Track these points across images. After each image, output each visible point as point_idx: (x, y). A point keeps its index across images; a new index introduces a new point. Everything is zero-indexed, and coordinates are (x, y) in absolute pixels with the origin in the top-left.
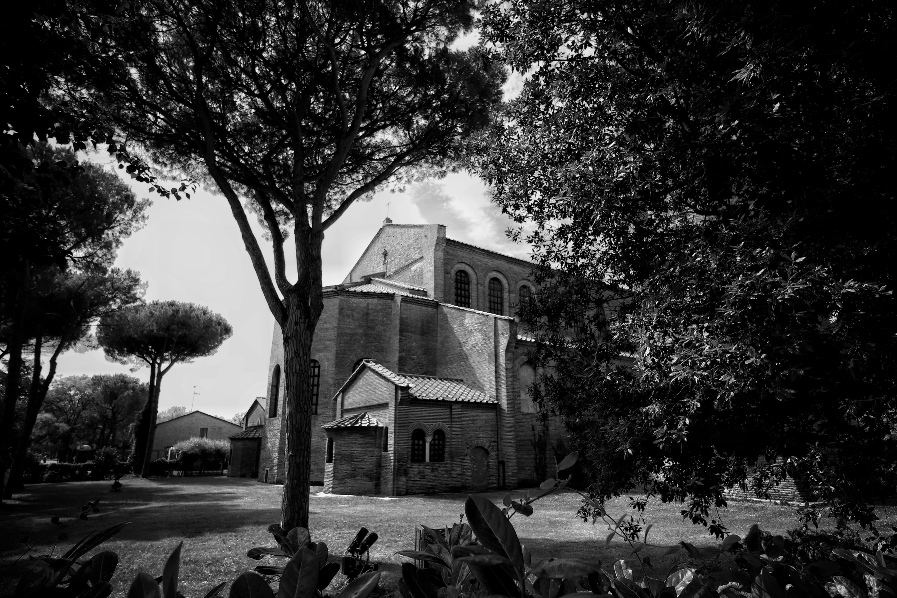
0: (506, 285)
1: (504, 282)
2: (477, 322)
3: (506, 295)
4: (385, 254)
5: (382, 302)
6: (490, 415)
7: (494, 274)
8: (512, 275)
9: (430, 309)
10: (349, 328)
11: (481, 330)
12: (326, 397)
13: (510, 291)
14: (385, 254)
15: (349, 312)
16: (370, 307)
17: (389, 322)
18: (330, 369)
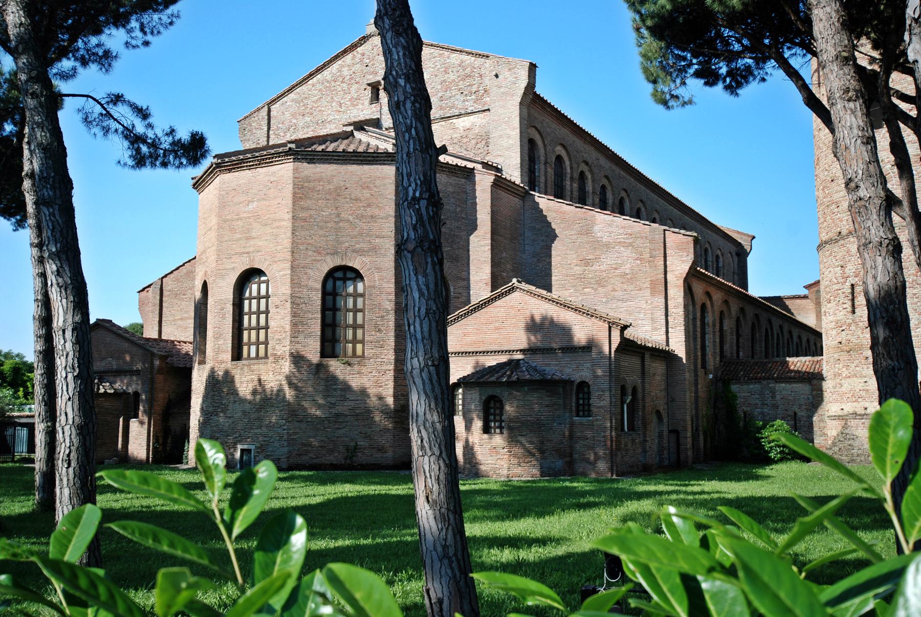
0: (569, 171)
2: (621, 231)
5: (453, 180)
7: (559, 150)
8: (575, 153)
9: (516, 200)
11: (631, 244)
12: (380, 330)
13: (572, 178)
17: (463, 215)
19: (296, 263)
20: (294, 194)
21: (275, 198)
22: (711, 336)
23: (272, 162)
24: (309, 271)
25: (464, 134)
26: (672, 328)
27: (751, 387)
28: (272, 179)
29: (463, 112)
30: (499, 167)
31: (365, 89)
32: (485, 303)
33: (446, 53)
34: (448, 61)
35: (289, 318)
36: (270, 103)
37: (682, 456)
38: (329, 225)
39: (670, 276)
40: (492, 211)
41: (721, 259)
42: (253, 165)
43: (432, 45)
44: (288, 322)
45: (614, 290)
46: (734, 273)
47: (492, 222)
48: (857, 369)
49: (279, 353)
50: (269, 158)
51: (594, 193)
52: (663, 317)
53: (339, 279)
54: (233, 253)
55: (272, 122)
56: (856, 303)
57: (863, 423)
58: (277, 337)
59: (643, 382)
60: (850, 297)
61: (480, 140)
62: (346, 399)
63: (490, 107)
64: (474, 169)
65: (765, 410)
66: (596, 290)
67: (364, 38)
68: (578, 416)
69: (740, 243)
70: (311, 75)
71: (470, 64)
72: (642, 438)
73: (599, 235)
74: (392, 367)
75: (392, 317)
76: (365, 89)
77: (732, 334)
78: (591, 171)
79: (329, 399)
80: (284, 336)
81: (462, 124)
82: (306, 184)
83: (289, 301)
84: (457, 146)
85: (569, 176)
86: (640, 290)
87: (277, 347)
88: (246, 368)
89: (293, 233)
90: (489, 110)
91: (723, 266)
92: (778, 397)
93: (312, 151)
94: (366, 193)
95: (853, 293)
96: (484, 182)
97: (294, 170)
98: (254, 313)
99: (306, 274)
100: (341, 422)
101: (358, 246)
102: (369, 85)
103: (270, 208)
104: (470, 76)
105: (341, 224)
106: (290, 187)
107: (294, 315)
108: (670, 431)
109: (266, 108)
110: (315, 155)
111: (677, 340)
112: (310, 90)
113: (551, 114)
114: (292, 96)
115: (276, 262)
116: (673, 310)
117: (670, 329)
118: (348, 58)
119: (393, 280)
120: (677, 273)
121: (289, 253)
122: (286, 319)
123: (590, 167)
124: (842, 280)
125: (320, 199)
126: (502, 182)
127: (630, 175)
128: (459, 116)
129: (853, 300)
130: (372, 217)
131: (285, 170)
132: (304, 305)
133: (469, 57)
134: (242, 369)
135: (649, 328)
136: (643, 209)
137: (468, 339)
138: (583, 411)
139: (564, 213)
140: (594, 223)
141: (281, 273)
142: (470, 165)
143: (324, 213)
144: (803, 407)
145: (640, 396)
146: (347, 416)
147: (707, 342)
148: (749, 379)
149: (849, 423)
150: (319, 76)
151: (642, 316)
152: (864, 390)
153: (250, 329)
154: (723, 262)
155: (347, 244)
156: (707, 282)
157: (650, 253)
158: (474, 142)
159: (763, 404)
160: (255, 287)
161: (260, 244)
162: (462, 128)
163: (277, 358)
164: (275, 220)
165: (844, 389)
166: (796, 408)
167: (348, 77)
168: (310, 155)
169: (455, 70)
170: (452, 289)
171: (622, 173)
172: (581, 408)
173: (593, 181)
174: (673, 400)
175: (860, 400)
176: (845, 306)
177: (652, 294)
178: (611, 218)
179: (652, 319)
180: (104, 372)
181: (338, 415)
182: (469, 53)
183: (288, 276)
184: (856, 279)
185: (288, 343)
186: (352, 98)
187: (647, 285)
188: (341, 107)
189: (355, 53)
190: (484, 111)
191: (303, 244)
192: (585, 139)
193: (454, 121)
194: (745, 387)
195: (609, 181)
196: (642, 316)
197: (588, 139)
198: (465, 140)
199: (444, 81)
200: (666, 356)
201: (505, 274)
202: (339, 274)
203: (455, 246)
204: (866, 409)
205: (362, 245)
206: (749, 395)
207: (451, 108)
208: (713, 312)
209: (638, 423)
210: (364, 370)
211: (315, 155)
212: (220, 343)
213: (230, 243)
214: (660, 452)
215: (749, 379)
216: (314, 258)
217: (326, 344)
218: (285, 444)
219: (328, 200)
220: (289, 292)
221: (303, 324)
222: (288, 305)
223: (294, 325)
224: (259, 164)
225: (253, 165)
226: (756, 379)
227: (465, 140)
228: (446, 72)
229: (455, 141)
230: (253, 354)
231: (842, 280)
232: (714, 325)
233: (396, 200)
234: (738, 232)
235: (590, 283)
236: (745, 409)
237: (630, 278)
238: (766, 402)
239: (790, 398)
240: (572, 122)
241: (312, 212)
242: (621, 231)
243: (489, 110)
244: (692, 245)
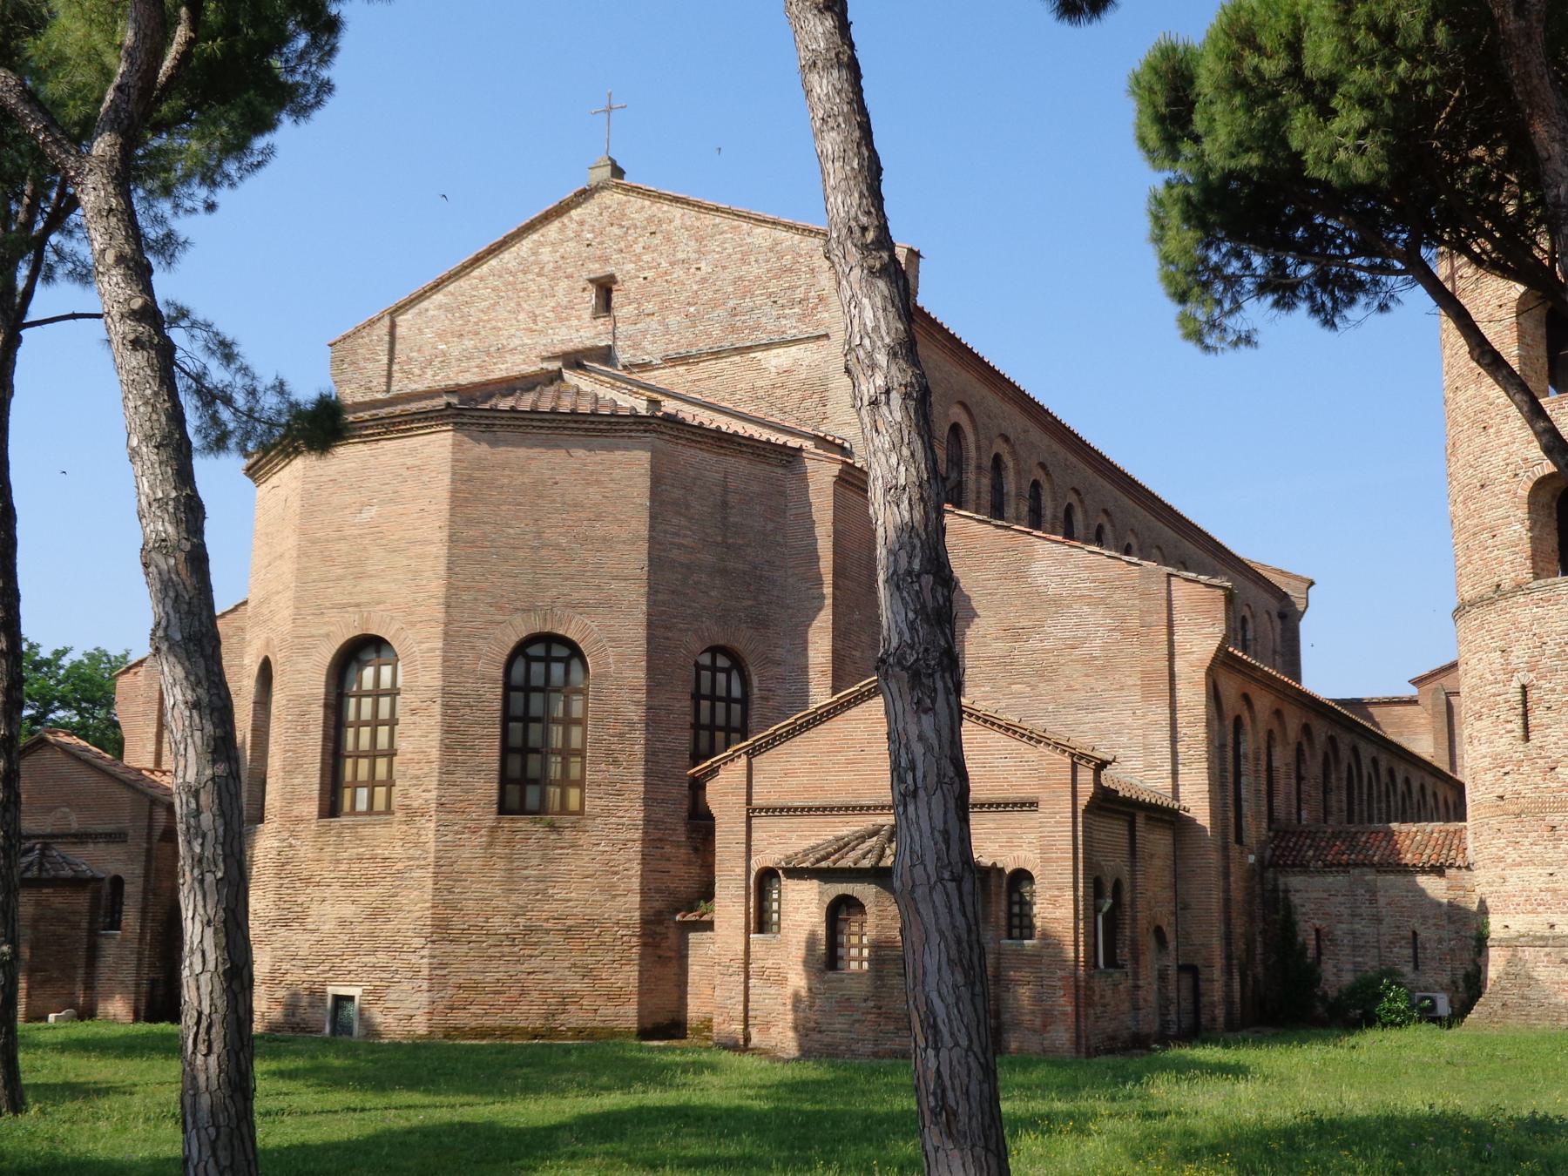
0: (973, 453)
1: (970, 438)
3: (971, 477)
4: (605, 288)
5: (760, 469)
6: (1157, 842)
10: (679, 546)
12: (615, 762)
13: (979, 467)
14: (605, 288)
15: (677, 493)
16: (732, 485)
17: (779, 538)
18: (628, 674)
19: (453, 627)
20: (454, 493)
21: (415, 498)
22: (1252, 779)
23: (408, 430)
24: (479, 643)
25: (779, 381)
26: (1184, 764)
27: (1330, 879)
28: (410, 461)
29: (776, 338)
30: (847, 445)
31: (584, 289)
32: (828, 711)
33: (745, 226)
34: (749, 240)
35: (436, 736)
36: (396, 311)
37: (1204, 1018)
38: (521, 554)
39: (1180, 665)
40: (835, 532)
41: (1250, 625)
42: (373, 435)
43: (717, 210)
44: (436, 744)
45: (1070, 689)
46: (1275, 652)
47: (835, 553)
48: (1537, 849)
49: (415, 804)
50: (406, 423)
51: (1019, 495)
52: (1167, 743)
53: (538, 659)
54: (328, 604)
55: (398, 347)
56: (1532, 722)
57: (1548, 954)
58: (412, 772)
59: (1133, 873)
60: (1520, 710)
61: (808, 393)
62: (549, 898)
63: (828, 331)
64: (800, 449)
66: (1033, 687)
67: (584, 192)
68: (1010, 937)
69: (1285, 593)
70: (478, 260)
71: (792, 248)
72: (1130, 982)
73: (1040, 580)
74: (638, 835)
75: (639, 736)
76: (584, 289)
78: (1014, 453)
79: (513, 897)
80: (426, 769)
81: (774, 362)
82: (477, 474)
83: (439, 701)
84: (764, 404)
85: (973, 463)
86: (1122, 688)
87: (413, 793)
88: (347, 834)
89: (449, 569)
90: (827, 336)
91: (1255, 639)
92: (1382, 901)
93: (491, 410)
94: (594, 493)
95: (1524, 702)
96: (822, 474)
97: (454, 445)
98: (366, 724)
99: (473, 648)
100: (535, 944)
101: (575, 595)
102: (591, 281)
103: (405, 518)
104: (790, 270)
105: (543, 552)
106: (446, 479)
107: (448, 729)
108: (1182, 969)
109: (386, 321)
110: (495, 418)
111: (1195, 788)
112: (476, 288)
113: (944, 346)
114: (439, 298)
115: (413, 624)
116: (1184, 731)
117: (1180, 767)
118: (552, 229)
119: (644, 663)
120: (1192, 657)
121: (441, 608)
122: (431, 736)
123: (1013, 446)
124: (1504, 677)
125: (505, 502)
126: (854, 476)
128: (769, 346)
129: (1525, 715)
130: (605, 540)
131: (437, 446)
132: (468, 710)
133: (789, 235)
134: (339, 835)
135: (1139, 764)
137: (793, 782)
138: (1021, 927)
139: (974, 537)
140: (1031, 559)
141: (424, 646)
142: (793, 442)
143: (511, 531)
144: (1431, 922)
145: (1126, 897)
146: (548, 931)
148: (1325, 866)
149: (1520, 954)
150: (493, 262)
151: (1125, 739)
152: (1547, 890)
153: (358, 755)
154: (1255, 631)
155: (554, 592)
156: (1244, 674)
157: (1141, 618)
158: (797, 396)
159: (1353, 915)
160: (368, 673)
161: (382, 587)
162: (773, 370)
163: (412, 814)
164: (413, 542)
165: (1509, 887)
166: (1416, 924)
167: (551, 265)
168: (487, 418)
169: (761, 257)
170: (755, 681)
171: (1071, 458)
172: (1016, 921)
173: (1018, 472)
174: (1185, 907)
175: (1540, 909)
176: (1509, 726)
177: (1147, 695)
178: (1064, 549)
179: (1145, 747)
180: (53, 836)
181: (530, 930)
182: (789, 227)
183: (438, 653)
184: (1532, 676)
185: (434, 785)
186: (559, 304)
187: (1134, 680)
188: (535, 322)
189: (565, 219)
190: (818, 338)
191: (468, 589)
192: (1004, 394)
193: (758, 355)
194: (1318, 881)
195: (1048, 474)
196: (1125, 739)
197: (1010, 392)
198: (779, 392)
199: (741, 278)
200: (1169, 818)
201: (858, 654)
202: (537, 650)
203: (763, 598)
204: (1552, 926)
205: (584, 593)
206: (1325, 895)
207: (753, 329)
209: (1123, 953)
210: (583, 839)
211: (495, 418)
212: (296, 781)
213: (322, 585)
214: (1163, 1008)
215: (1325, 866)
216: (489, 617)
217: (509, 787)
218: (425, 986)
219: (520, 504)
220: (438, 683)
221: (465, 748)
222: (437, 708)
223: (447, 748)
224: (385, 433)
225: (373, 435)
226: (1340, 864)
227: (779, 392)
228: (744, 261)
229: (761, 393)
230: (362, 805)
231: (1504, 677)
232: (1257, 759)
233: (651, 507)
234: (1282, 573)
235: (1023, 673)
236: (1318, 923)
237: (1104, 667)
238: (1359, 911)
240: (981, 360)
241: (488, 528)
242: (1085, 575)
243: (827, 336)
244: (1222, 605)
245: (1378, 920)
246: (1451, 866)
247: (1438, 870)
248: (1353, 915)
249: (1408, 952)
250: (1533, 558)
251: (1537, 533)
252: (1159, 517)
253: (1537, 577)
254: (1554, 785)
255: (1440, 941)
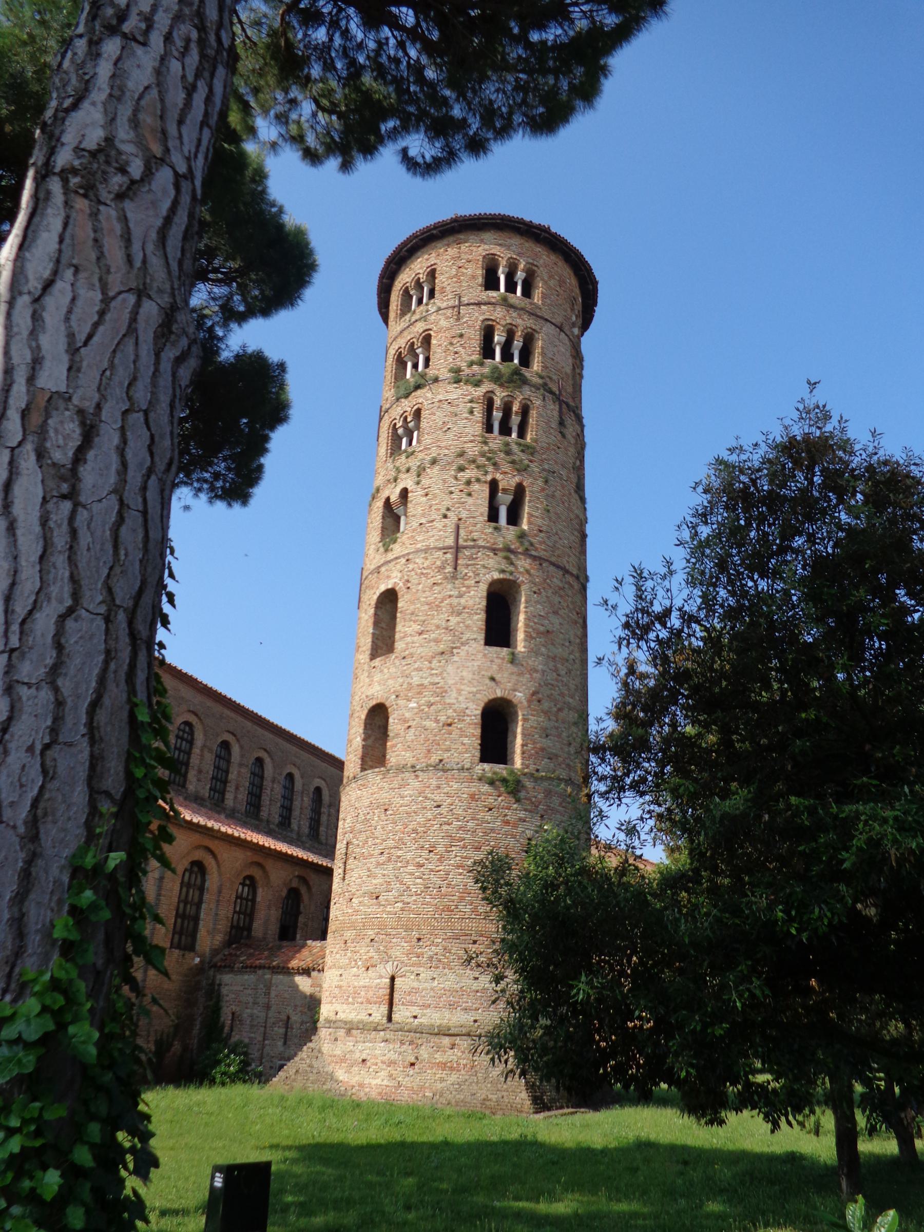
22: (213, 906)
27: (246, 977)
48: (338, 956)
56: (348, 867)
65: (255, 1011)
77: (269, 908)
92: (273, 994)
127: (246, 718)
136: (267, 760)
144: (299, 1009)
147: (202, 914)
156: (200, 832)
159: (254, 1003)
166: (290, 1010)
175: (334, 1000)
184: (351, 835)
195: (200, 719)
206: (241, 988)
208: (220, 874)
226: (251, 967)
236: (234, 1008)
239: (286, 995)
245: (268, 1007)
246: (314, 970)
247: (307, 972)
248: (254, 1003)
249: (282, 1031)
250: (363, 759)
251: (370, 742)
252: (324, 761)
253: (363, 769)
254: (350, 911)
255: (302, 1023)
